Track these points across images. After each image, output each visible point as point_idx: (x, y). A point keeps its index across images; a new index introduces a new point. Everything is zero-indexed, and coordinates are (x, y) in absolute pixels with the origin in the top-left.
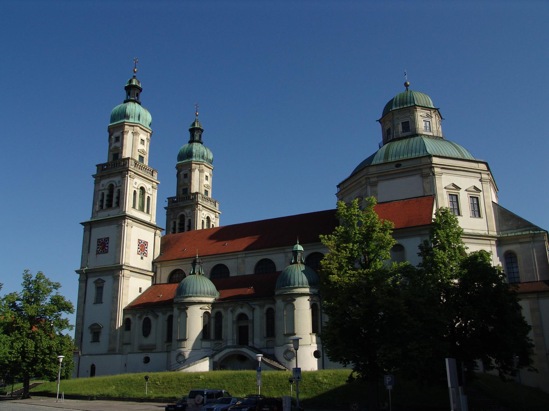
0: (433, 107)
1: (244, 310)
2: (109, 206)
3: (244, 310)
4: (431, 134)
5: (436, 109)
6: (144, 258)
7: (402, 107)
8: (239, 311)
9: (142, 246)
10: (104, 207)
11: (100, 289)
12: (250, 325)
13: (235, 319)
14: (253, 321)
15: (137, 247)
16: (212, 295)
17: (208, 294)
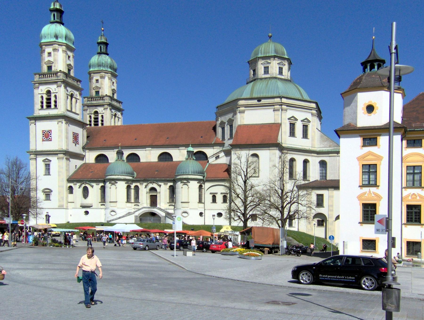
0: (287, 57)
1: (155, 186)
2: (49, 106)
3: (155, 186)
4: (283, 77)
5: (288, 60)
6: (77, 145)
7: (265, 56)
8: (151, 186)
9: (76, 137)
10: (45, 107)
11: (48, 167)
12: (158, 195)
13: (148, 191)
14: (160, 192)
15: (72, 137)
16: (131, 174)
17: (129, 174)
